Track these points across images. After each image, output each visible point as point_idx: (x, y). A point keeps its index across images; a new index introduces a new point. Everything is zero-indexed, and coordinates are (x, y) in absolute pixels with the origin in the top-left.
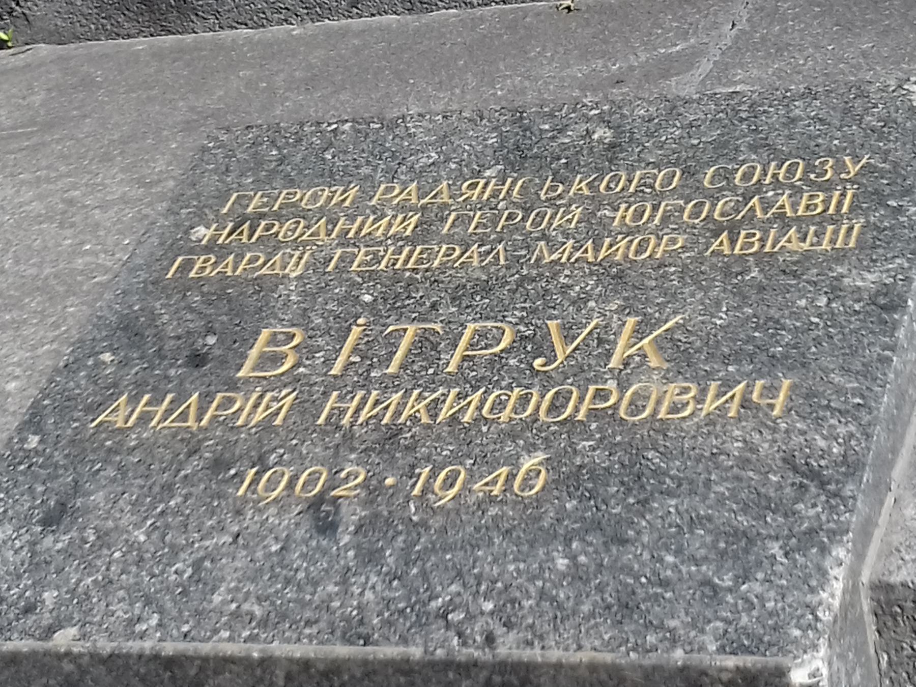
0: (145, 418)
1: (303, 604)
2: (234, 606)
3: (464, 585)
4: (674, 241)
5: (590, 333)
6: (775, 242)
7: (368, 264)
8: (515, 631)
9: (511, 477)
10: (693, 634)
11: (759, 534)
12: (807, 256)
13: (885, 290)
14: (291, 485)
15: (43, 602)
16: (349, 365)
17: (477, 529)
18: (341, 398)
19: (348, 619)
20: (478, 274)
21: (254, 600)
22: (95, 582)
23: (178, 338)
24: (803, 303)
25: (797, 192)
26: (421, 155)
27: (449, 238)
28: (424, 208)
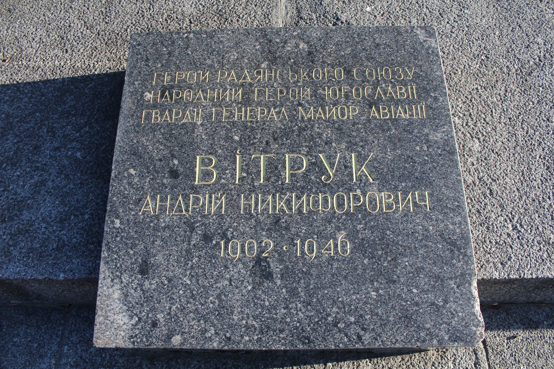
0: (163, 209)
1: (275, 320)
2: (244, 322)
3: (338, 308)
4: (354, 110)
5: (339, 162)
6: (395, 114)
7: (229, 118)
9: (336, 246)
11: (444, 277)
14: (243, 251)
15: (159, 320)
16: (242, 179)
17: (333, 275)
18: (246, 198)
19: (297, 328)
20: (279, 125)
21: (252, 318)
23: (161, 160)
24: (418, 148)
25: (394, 86)
26: (230, 54)
27: (259, 104)
28: (242, 85)
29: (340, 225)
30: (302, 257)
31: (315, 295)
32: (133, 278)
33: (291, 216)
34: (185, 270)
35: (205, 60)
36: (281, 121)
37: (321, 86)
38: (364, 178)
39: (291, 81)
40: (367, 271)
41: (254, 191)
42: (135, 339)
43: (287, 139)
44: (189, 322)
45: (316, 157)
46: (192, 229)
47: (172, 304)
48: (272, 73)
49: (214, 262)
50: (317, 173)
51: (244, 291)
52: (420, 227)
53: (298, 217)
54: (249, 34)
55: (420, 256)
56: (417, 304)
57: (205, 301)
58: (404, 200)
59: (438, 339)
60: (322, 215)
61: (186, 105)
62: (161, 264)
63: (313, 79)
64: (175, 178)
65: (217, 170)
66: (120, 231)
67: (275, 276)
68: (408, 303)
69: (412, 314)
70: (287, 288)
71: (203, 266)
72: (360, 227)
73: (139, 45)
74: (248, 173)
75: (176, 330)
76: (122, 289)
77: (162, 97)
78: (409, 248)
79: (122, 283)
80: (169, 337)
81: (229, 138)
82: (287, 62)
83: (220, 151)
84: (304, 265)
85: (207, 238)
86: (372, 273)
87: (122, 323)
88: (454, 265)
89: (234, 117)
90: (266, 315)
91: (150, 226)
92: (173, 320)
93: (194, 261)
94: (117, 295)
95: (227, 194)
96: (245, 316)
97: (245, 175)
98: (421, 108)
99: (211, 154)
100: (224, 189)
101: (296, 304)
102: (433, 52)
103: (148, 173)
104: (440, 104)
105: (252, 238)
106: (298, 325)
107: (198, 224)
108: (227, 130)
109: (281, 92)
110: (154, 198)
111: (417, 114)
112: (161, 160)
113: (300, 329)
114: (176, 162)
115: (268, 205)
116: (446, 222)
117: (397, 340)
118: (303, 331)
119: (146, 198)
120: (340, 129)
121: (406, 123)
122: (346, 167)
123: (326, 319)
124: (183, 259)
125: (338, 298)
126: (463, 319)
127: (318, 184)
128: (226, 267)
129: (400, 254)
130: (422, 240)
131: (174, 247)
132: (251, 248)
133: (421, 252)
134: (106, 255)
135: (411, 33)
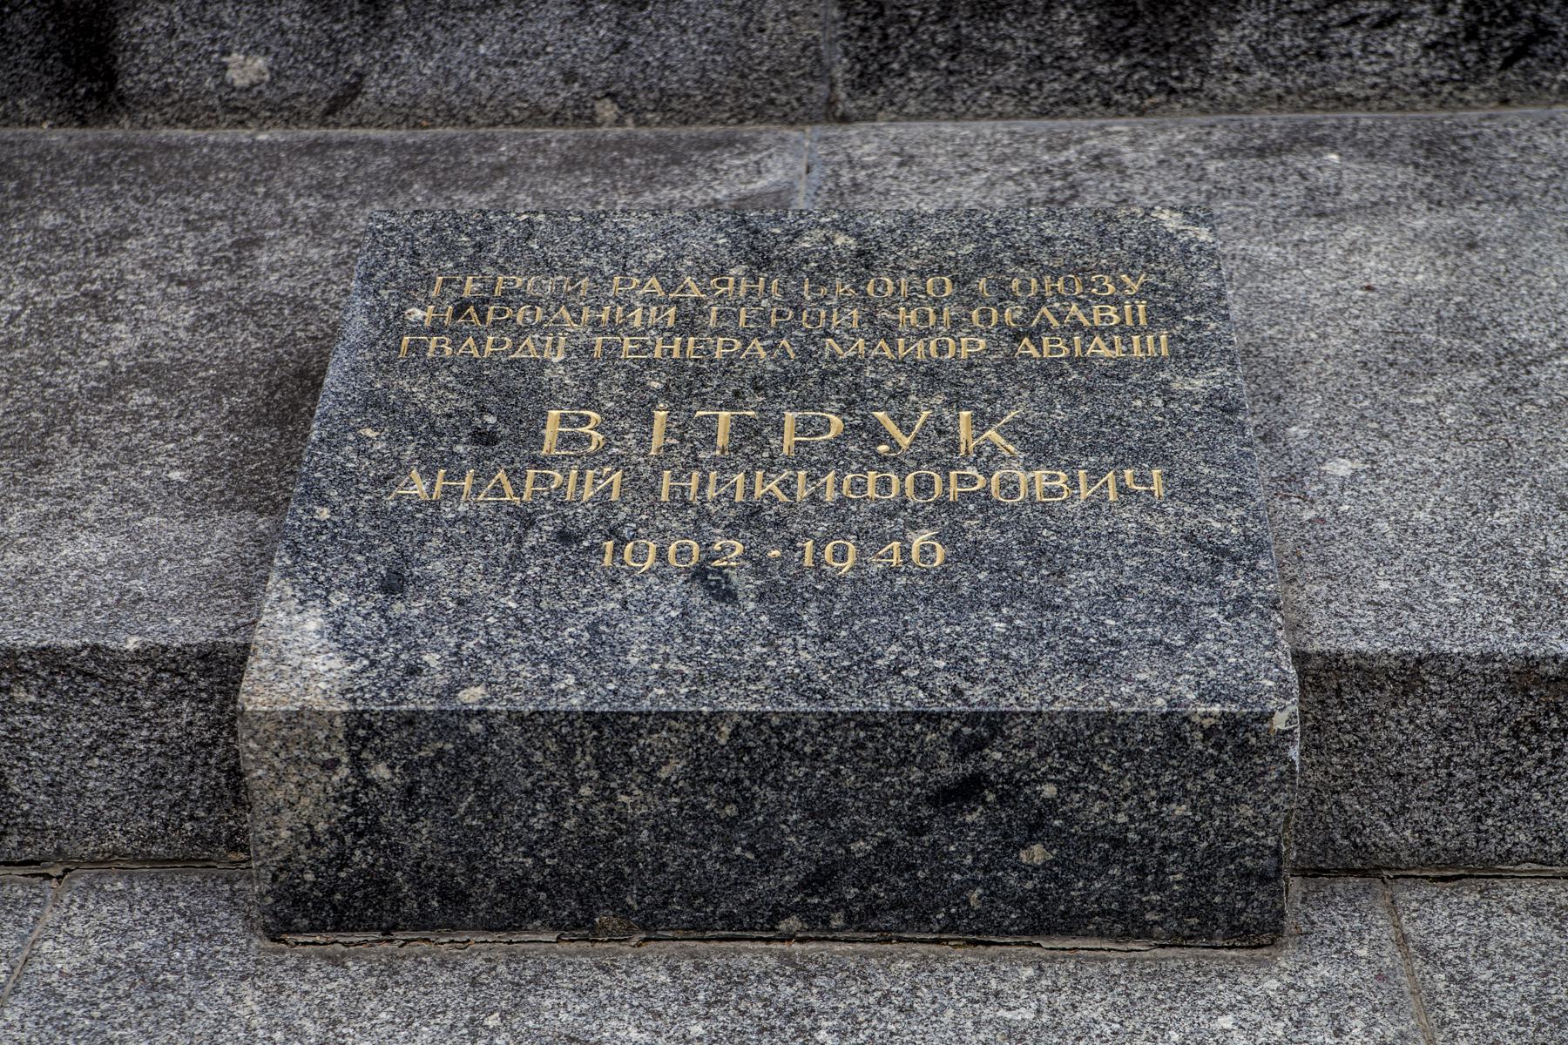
0: (452, 493)
1: (736, 665)
5: (925, 424)
6: (1084, 350)
10: (1166, 685)
12: (1123, 364)
19: (792, 676)
20: (770, 367)
23: (449, 416)
24: (1139, 403)
25: (1084, 305)
27: (718, 332)
28: (676, 302)
32: (362, 598)
34: (506, 586)
35: (576, 258)
36: (774, 361)
43: (788, 389)
48: (757, 282)
54: (699, 219)
61: (521, 332)
65: (602, 432)
67: (740, 597)
73: (391, 229)
74: (682, 439)
78: (1099, 557)
80: (451, 690)
84: (819, 579)
85: (564, 537)
94: (313, 622)
98: (1157, 340)
102: (1200, 249)
108: (631, 372)
109: (780, 314)
110: (430, 474)
116: (1202, 518)
117: (1057, 698)
118: (810, 680)
120: (932, 376)
121: (1111, 364)
126: (1237, 668)
127: (866, 457)
128: (614, 582)
132: (680, 553)
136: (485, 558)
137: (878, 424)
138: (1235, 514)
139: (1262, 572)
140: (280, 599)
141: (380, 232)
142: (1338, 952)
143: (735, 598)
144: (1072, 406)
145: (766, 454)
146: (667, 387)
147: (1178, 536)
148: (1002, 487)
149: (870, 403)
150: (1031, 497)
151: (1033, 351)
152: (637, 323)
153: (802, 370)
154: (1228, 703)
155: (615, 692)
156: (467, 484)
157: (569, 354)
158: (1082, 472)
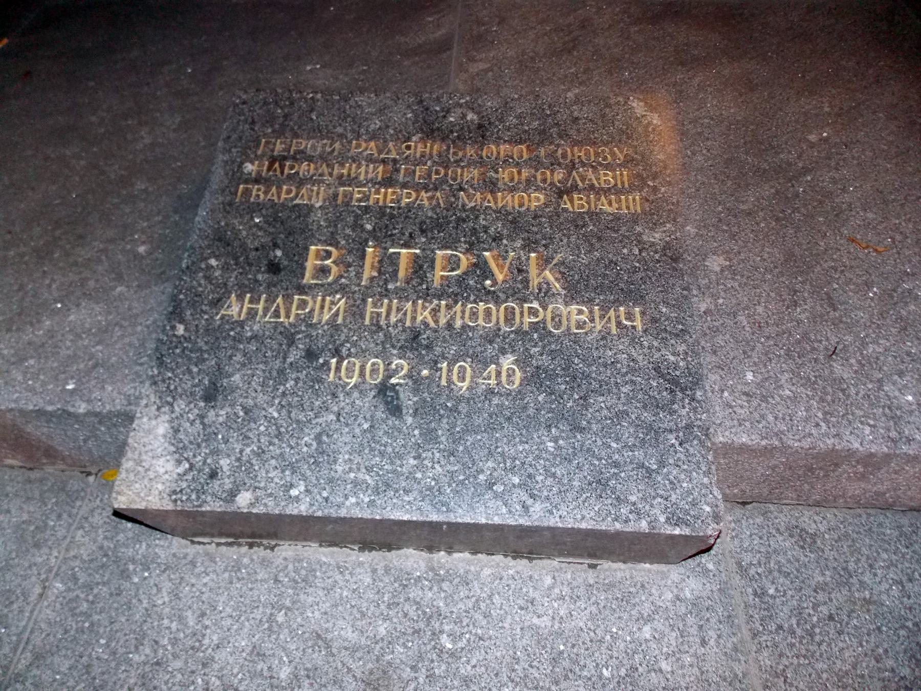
0: (252, 314)
6: (596, 206)
8: (539, 503)
9: (499, 374)
13: (667, 246)
14: (362, 374)
18: (375, 305)
19: (430, 489)
21: (364, 471)
22: (253, 451)
23: (257, 249)
24: (625, 251)
27: (404, 186)
28: (383, 161)
29: (507, 346)
30: (448, 387)
31: (462, 442)
32: (192, 406)
33: (436, 331)
34: (273, 397)
35: (335, 127)
36: (433, 209)
37: (492, 168)
38: (545, 286)
39: (452, 160)
40: (543, 412)
41: (386, 296)
42: (179, 496)
43: (439, 232)
44: (267, 472)
45: (478, 256)
46: (292, 342)
47: (244, 445)
49: (317, 387)
50: (478, 276)
51: (357, 431)
52: (625, 356)
53: (446, 332)
54: (399, 99)
55: (622, 395)
56: (616, 465)
57: (297, 443)
58: (602, 317)
59: (649, 519)
60: (481, 332)
62: (237, 388)
63: (482, 158)
64: (275, 273)
65: (337, 265)
66: (182, 339)
67: (404, 411)
68: (604, 461)
69: (609, 479)
70: (421, 429)
71: (300, 393)
72: (534, 350)
73: (244, 103)
74: (380, 272)
75: (245, 484)
76: (171, 421)
77: (269, 170)
79: (172, 412)
80: (232, 494)
81: (357, 226)
82: (448, 136)
83: (343, 242)
85: (311, 355)
86: (550, 415)
87: (162, 470)
88: (675, 412)
89: (368, 200)
90: (386, 467)
91: (229, 335)
92: (243, 468)
93: (288, 386)
94: (162, 428)
95: (348, 298)
96: (354, 467)
97: (375, 274)
99: (330, 245)
100: (343, 289)
101: (433, 453)
102: (654, 130)
103: (236, 264)
104: (660, 195)
105: (377, 357)
106: (433, 483)
107: (300, 336)
108: (357, 217)
110: (240, 298)
111: (628, 208)
112: (257, 249)
113: (435, 490)
114: (279, 253)
115: (405, 314)
116: (663, 352)
119: (229, 298)
120: (515, 222)
121: (610, 218)
122: (520, 271)
123: (475, 478)
124: (271, 382)
125: (497, 447)
126: (689, 493)
127: (479, 291)
128: (334, 395)
129: (592, 391)
130: (627, 373)
131: (261, 366)
132: (374, 371)
133: (624, 390)
134: (156, 372)
135: (624, 105)
136: (264, 371)
137: (486, 262)
138: (682, 348)
139: (699, 402)
140: (147, 406)
141: (237, 105)
142: (699, 565)
143: (401, 413)
144: (590, 252)
145: (424, 286)
146: (374, 229)
147: (651, 366)
148: (553, 319)
149: (482, 245)
150: (569, 329)
151: (568, 206)
152: (362, 177)
153: (447, 217)
154: (684, 527)
155: (327, 499)
156: (260, 306)
157: (324, 200)
158: (596, 308)
